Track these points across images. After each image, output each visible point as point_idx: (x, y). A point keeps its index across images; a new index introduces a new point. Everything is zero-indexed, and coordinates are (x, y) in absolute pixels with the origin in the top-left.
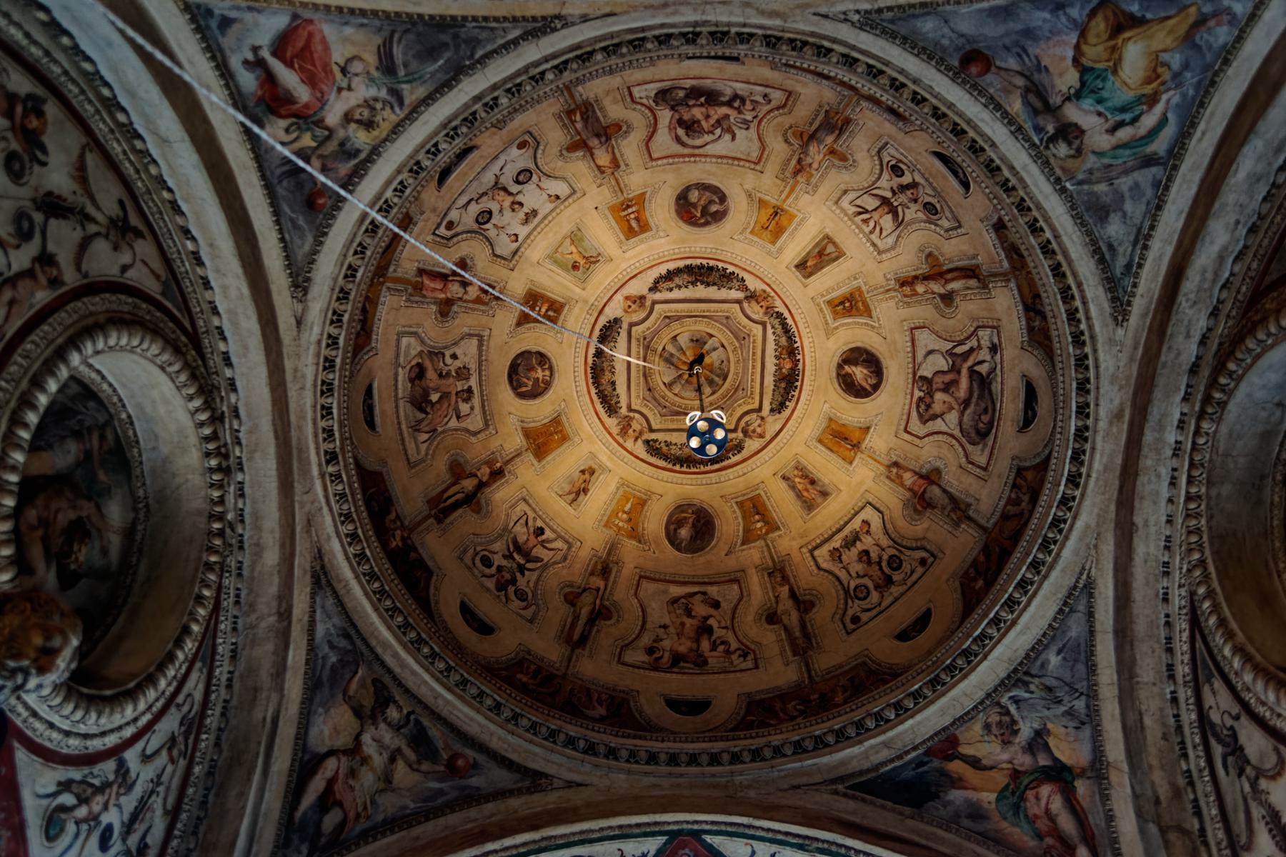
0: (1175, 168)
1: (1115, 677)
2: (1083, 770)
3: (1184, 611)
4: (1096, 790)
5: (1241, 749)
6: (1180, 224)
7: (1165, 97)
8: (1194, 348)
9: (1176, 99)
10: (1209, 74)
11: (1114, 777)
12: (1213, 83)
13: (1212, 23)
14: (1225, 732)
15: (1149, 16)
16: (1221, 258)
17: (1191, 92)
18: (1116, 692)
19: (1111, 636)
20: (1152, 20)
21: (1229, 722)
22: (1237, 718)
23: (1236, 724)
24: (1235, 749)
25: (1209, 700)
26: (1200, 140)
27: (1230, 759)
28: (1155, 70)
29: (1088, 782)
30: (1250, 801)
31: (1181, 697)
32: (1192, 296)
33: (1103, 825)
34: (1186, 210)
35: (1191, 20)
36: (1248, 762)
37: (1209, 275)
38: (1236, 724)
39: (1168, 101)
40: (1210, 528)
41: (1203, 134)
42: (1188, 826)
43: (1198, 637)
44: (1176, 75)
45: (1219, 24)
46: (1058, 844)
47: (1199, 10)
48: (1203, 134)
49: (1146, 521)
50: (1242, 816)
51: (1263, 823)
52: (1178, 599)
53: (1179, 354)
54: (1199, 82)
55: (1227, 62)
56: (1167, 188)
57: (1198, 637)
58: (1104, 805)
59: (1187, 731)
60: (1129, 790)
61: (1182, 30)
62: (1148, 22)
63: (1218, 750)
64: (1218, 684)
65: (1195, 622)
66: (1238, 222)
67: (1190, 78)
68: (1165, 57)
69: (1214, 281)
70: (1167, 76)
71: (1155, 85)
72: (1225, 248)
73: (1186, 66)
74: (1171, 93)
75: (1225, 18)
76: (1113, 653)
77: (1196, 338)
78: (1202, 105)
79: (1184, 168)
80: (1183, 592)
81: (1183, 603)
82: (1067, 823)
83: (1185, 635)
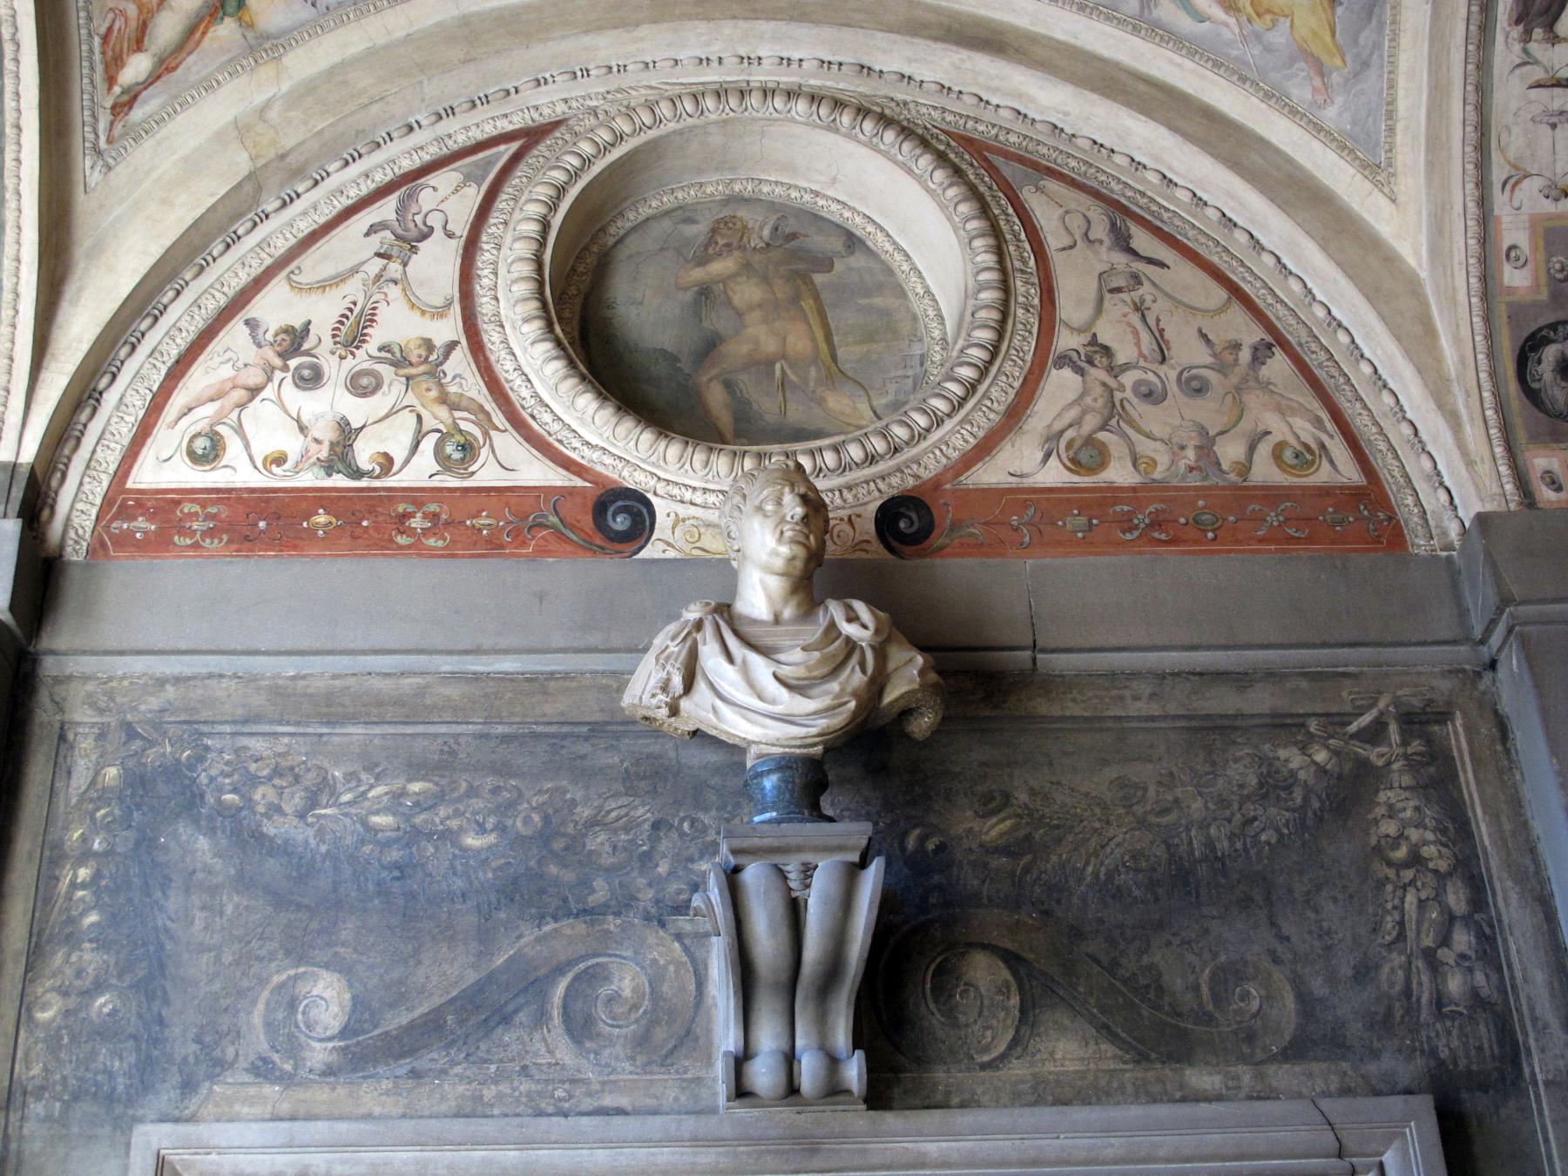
0: (1136, 30)
1: (400, 34)
2: (251, 26)
3: (536, 116)
4: (233, 54)
5: (414, 250)
6: (1059, 35)
7: (1232, 21)
8: (895, 68)
9: (1227, 34)
10: (1254, 75)
11: (266, 71)
12: (1243, 79)
13: (1317, 82)
14: (418, 219)
15: (1339, 10)
16: (1019, 96)
17: (1235, 53)
18: (381, 41)
19: (455, 13)
20: (1334, 13)
21: (435, 221)
22: (450, 235)
23: (438, 233)
24: (411, 239)
25: (444, 180)
26: (1171, 61)
27: (388, 234)
28: (1269, 11)
29: (238, 36)
30: (358, 277)
31: (418, 137)
32: (968, 65)
33: (193, 78)
34: (1079, 43)
35: (1325, 58)
36: (405, 265)
37: (996, 83)
38: (438, 233)
39: (1226, 25)
40: (667, 136)
41: (1179, 66)
42: (264, 196)
43: (514, 146)
44: (1258, 37)
45: (1315, 90)
46: (133, 24)
47: (1337, 69)
48: (1179, 66)
49: (642, 39)
50: (328, 270)
51: (347, 303)
52: (545, 103)
53: (885, 52)
54: (1247, 64)
55: (1268, 96)
56: (1108, 18)
57: (514, 146)
58: (220, 69)
59: (379, 157)
60: (259, 99)
61: (1316, 49)
62: (1333, 9)
63: (386, 209)
64: (473, 196)
65: (532, 136)
66: (1066, 114)
67: (1252, 53)
68: (1284, 24)
69: (989, 89)
70: (1258, 25)
71: (1250, 10)
72: (1033, 100)
73: (1268, 49)
74: (1237, 30)
75: (1320, 99)
76: (431, 22)
77: (907, 71)
78: (1217, 65)
79: (1135, 41)
80: (561, 108)
81: (546, 111)
82: (167, 29)
83: (505, 126)
